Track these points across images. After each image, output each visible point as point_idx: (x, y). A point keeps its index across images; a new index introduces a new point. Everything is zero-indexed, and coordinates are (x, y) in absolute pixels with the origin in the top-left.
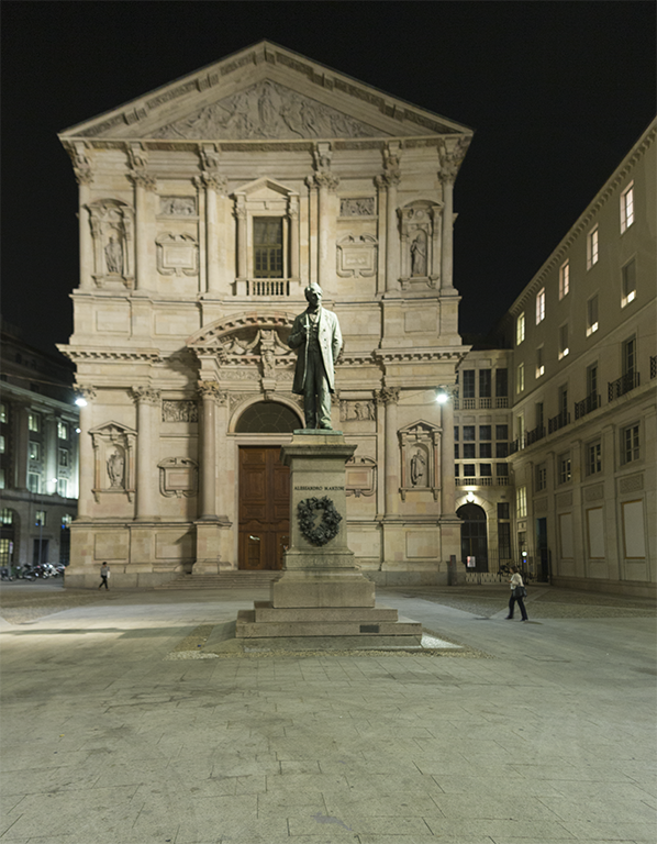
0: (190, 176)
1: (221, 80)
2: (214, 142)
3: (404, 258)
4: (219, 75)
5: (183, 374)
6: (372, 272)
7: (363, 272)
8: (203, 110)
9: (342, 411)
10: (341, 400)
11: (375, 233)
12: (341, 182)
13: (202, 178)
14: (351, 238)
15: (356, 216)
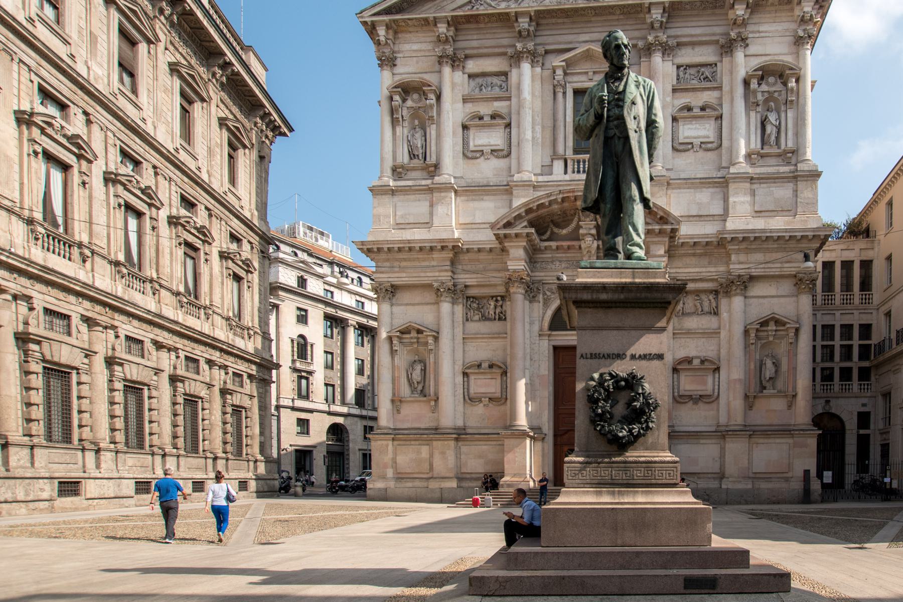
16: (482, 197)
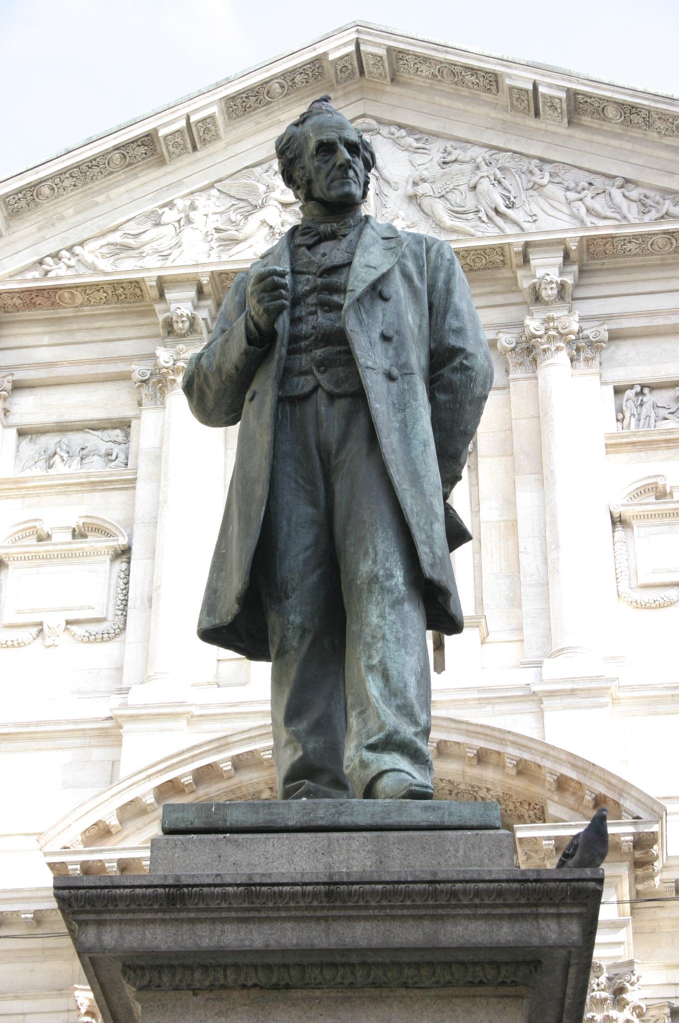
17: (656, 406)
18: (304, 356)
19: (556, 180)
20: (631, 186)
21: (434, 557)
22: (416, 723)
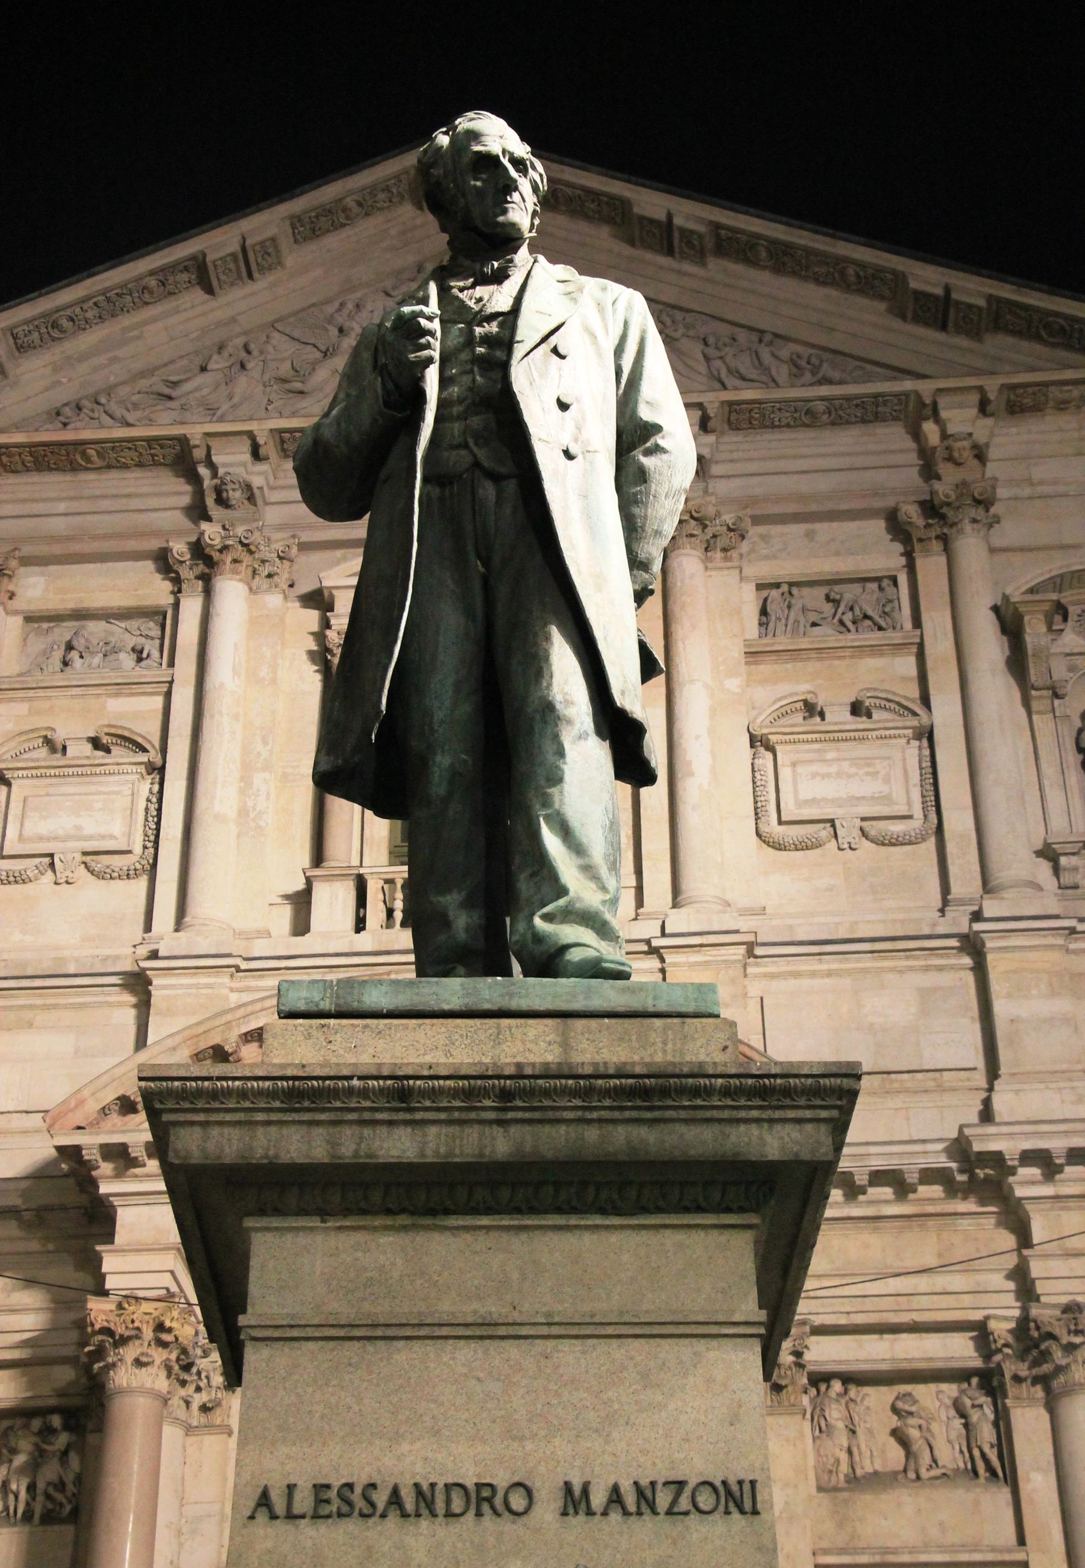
0: (155, 544)
1: (292, 258)
2: (253, 426)
3: (1050, 770)
4: (285, 243)
5: (30, 1282)
6: (917, 823)
7: (873, 828)
8: (221, 348)
9: (822, 1429)
10: (819, 1379)
11: (914, 692)
12: (754, 531)
13: (199, 550)
14: (811, 709)
15: (827, 636)
16: (28, 1015)
17: (804, 610)
18: (457, 425)
19: (692, 333)
20: (779, 342)
21: (625, 682)
22: (604, 889)
